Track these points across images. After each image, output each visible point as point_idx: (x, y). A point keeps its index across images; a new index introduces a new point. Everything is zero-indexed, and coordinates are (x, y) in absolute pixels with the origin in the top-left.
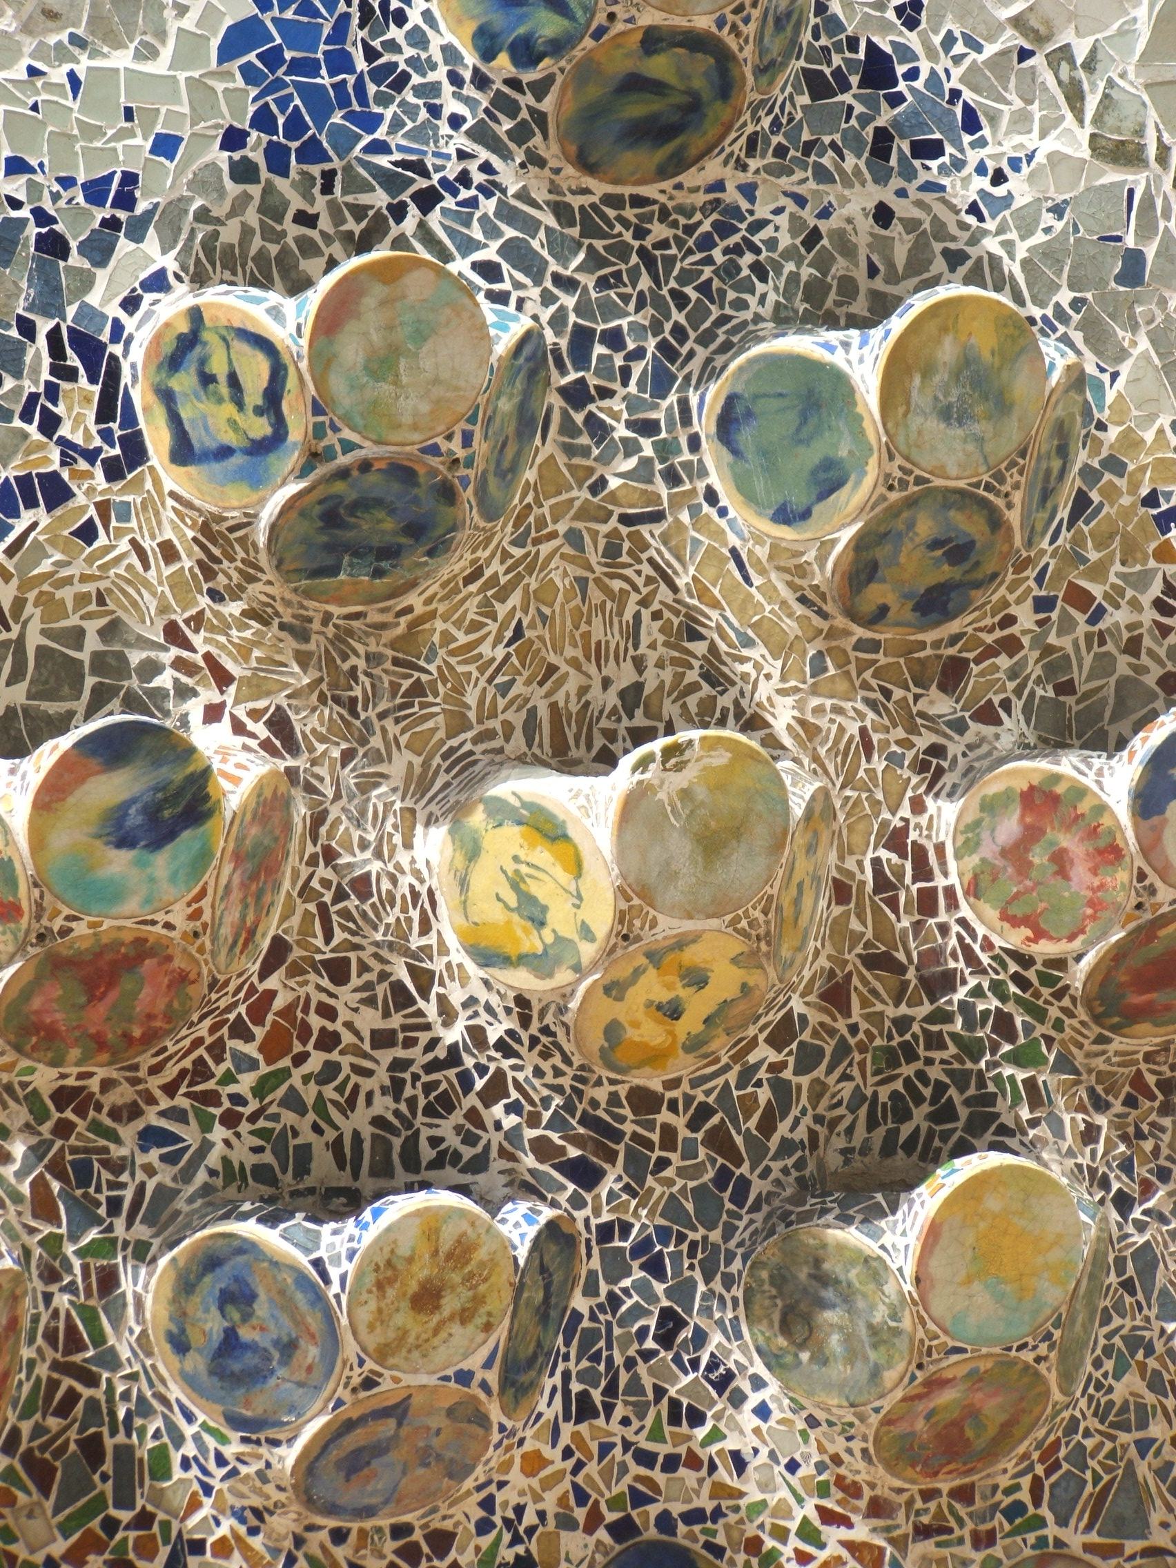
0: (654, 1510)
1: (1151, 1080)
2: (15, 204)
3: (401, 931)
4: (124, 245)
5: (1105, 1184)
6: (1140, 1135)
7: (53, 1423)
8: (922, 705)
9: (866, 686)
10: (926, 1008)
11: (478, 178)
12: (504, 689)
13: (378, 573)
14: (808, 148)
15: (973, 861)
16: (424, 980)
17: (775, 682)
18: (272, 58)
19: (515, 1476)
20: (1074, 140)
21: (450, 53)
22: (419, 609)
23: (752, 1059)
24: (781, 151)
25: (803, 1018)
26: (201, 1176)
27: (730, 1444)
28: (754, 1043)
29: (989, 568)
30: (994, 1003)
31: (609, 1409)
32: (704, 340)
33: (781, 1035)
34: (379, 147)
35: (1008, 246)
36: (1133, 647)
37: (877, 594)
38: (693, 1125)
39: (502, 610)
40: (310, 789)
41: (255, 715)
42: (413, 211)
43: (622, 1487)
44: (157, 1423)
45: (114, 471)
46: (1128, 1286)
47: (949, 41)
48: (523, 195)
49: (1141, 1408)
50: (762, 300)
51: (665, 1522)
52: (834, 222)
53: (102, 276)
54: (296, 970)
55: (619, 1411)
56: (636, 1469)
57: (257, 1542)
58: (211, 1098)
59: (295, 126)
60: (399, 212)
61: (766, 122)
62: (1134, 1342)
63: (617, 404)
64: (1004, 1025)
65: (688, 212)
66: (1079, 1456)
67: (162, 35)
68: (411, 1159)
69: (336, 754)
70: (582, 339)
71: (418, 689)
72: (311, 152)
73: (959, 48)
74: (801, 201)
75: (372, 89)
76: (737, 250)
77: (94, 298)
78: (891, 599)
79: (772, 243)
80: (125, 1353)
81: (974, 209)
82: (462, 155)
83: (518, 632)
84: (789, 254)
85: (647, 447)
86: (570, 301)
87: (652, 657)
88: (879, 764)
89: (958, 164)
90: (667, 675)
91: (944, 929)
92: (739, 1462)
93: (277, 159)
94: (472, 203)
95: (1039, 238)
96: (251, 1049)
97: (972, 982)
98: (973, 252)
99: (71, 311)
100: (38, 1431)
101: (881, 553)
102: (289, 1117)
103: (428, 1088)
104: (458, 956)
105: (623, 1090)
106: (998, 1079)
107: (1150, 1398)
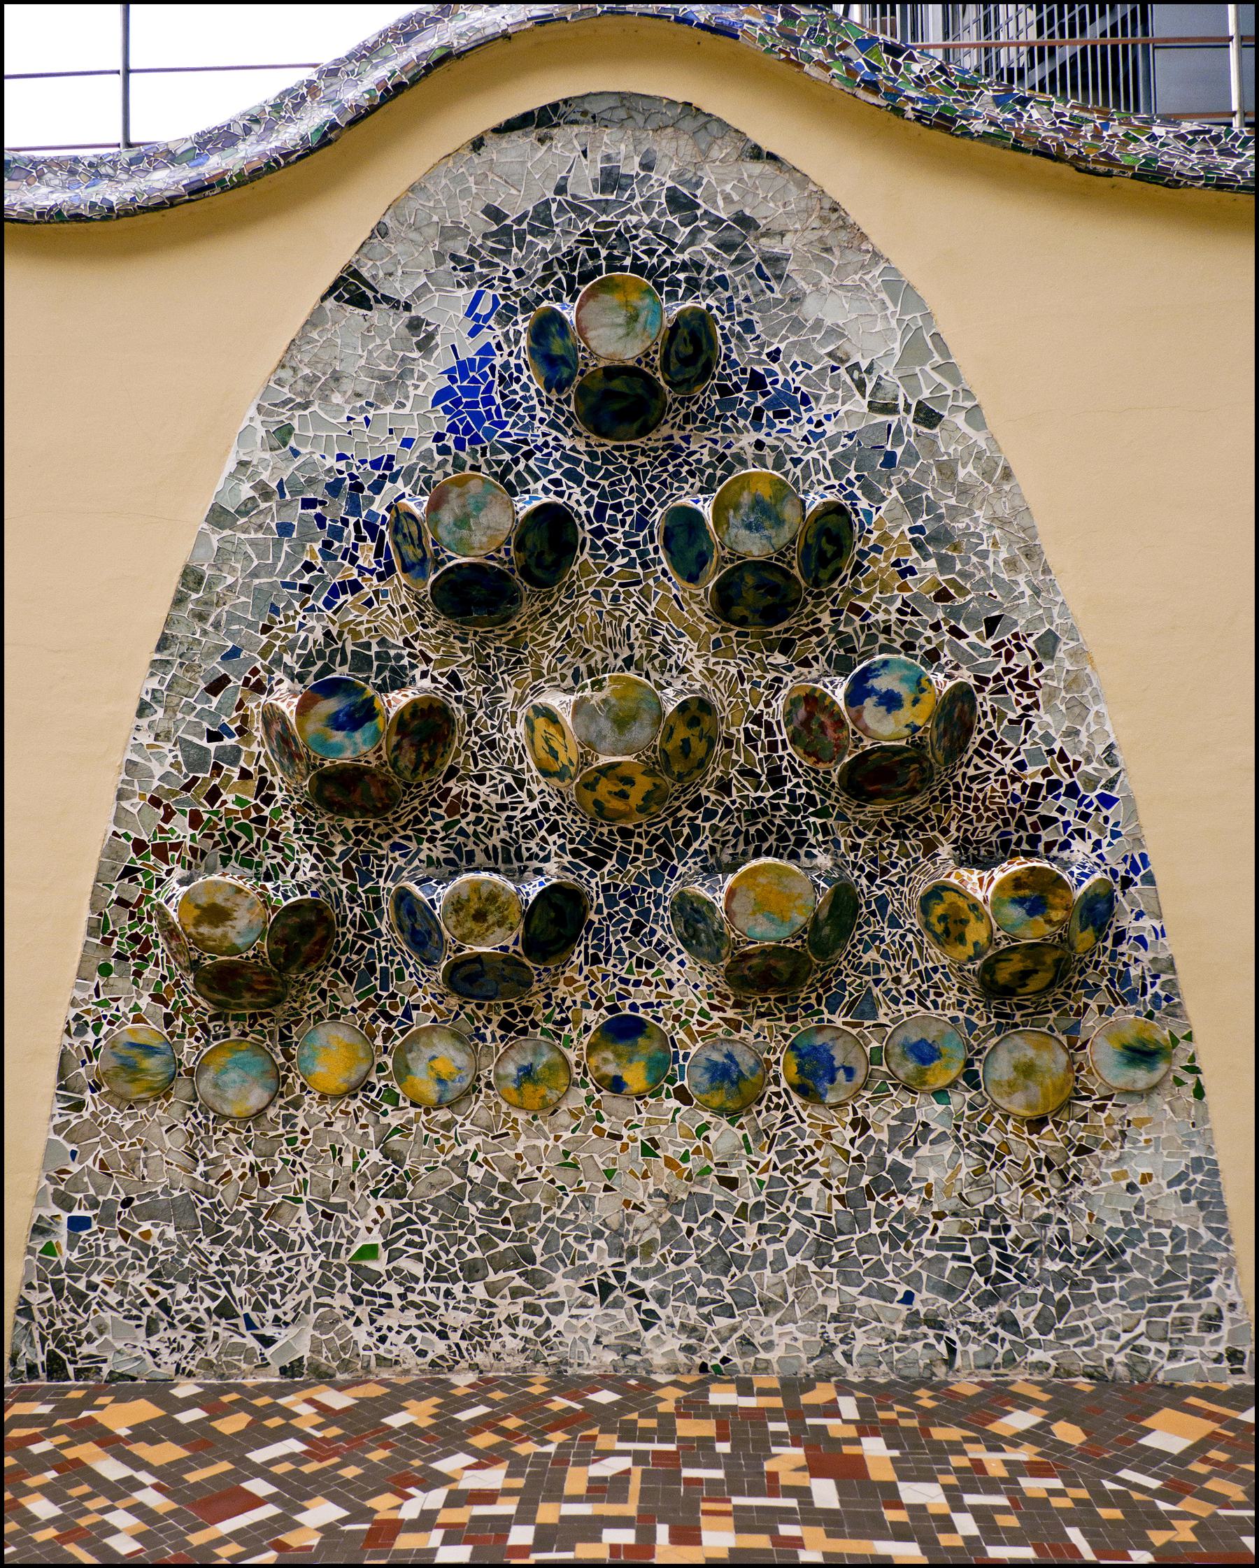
0: (628, 1002)
1: (889, 823)
2: (341, 472)
3: (510, 763)
4: (388, 485)
5: (861, 869)
6: (882, 847)
7: (355, 957)
8: (771, 660)
9: (741, 652)
10: (772, 793)
11: (552, 443)
12: (560, 660)
13: (490, 613)
14: (718, 418)
15: (791, 728)
16: (521, 783)
17: (695, 652)
18: (457, 403)
19: (561, 986)
20: (860, 404)
21: (537, 391)
22: (519, 628)
23: (679, 815)
24: (703, 420)
25: (707, 799)
26: (416, 862)
27: (667, 976)
28: (679, 808)
29: (793, 596)
30: (805, 790)
31: (607, 961)
32: (661, 506)
33: (696, 804)
34: (508, 435)
35: (823, 454)
36: (887, 630)
37: (738, 611)
38: (650, 843)
39: (560, 626)
40: (466, 704)
41: (442, 674)
42: (522, 460)
43: (614, 992)
44: (398, 959)
45: (381, 577)
46: (873, 913)
47: (795, 365)
48: (573, 449)
49: (876, 966)
50: (692, 486)
51: (634, 1007)
52: (734, 450)
53: (378, 498)
54: (460, 779)
55: (612, 962)
56: (619, 985)
57: (441, 1007)
58: (423, 831)
59: (468, 429)
60: (516, 461)
61: (695, 408)
62: (874, 937)
63: (619, 535)
64: (811, 800)
65: (655, 450)
66: (842, 986)
67: (407, 398)
68: (519, 857)
69: (480, 689)
70: (600, 511)
71: (519, 661)
72: (476, 440)
73: (800, 368)
74: (715, 442)
75: (503, 411)
76: (681, 465)
77: (374, 508)
78: (746, 613)
79: (699, 461)
80: (384, 931)
81: (805, 439)
82: (544, 435)
83: (568, 635)
84: (708, 465)
85: (633, 553)
86: (595, 493)
87: (637, 644)
88: (747, 686)
89: (798, 420)
90: (644, 651)
91: (781, 758)
92: (670, 984)
93: (460, 444)
94: (550, 454)
95: (840, 449)
96: (441, 812)
97: (795, 781)
98: (805, 458)
99: (364, 514)
100: (348, 959)
101: (732, 592)
102: (460, 839)
103: (523, 827)
104: (535, 773)
105: (615, 829)
106: (807, 824)
107: (881, 961)
